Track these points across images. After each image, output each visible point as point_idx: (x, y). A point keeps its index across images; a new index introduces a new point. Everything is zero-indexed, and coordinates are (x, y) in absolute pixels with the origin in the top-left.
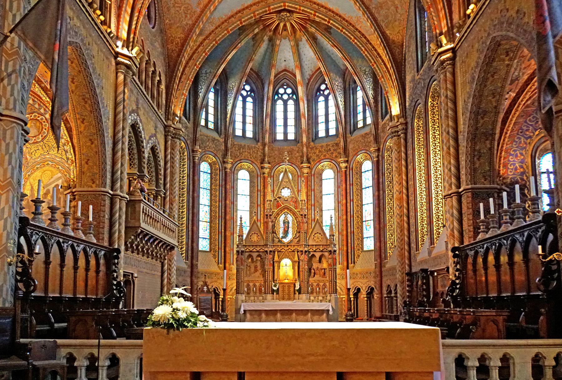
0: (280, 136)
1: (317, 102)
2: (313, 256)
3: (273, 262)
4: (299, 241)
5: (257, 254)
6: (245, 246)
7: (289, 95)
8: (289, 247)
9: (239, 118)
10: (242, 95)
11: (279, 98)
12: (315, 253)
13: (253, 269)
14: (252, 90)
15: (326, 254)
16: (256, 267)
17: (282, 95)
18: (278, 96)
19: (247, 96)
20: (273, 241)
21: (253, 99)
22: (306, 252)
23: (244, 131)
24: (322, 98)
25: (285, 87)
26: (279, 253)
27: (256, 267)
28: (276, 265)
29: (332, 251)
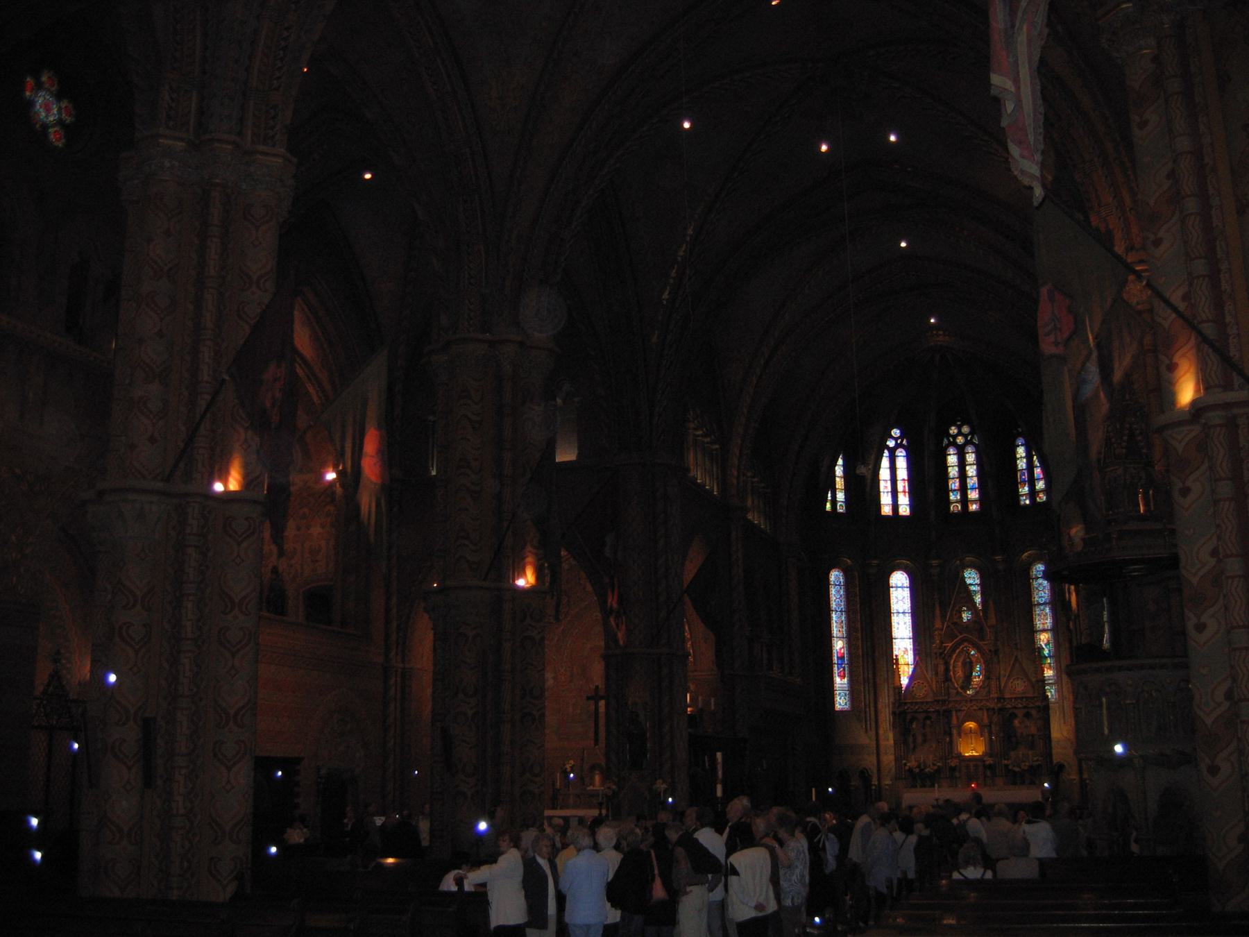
0: (956, 508)
2: (1013, 716)
3: (950, 728)
4: (989, 692)
6: (905, 704)
8: (974, 703)
9: (885, 486)
10: (888, 448)
13: (920, 739)
14: (902, 437)
17: (955, 437)
18: (949, 440)
19: (897, 446)
20: (948, 694)
22: (1000, 710)
23: (895, 506)
24: (1020, 441)
25: (959, 423)
26: (959, 714)
27: (925, 735)
28: (955, 731)
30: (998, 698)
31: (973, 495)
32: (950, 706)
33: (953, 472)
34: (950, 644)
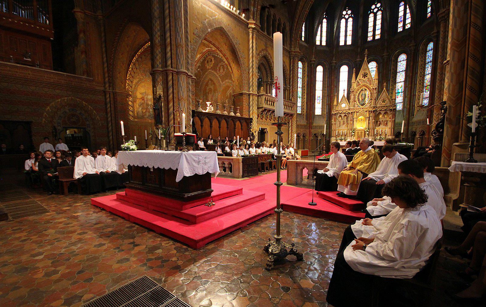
1: (399, 7)
2: (380, 113)
4: (371, 105)
5: (344, 114)
6: (337, 110)
7: (378, 8)
8: (364, 109)
11: (371, 13)
12: (381, 112)
13: (342, 123)
14: (351, 14)
15: (389, 112)
16: (344, 122)
18: (371, 11)
20: (354, 106)
21: (353, 19)
26: (357, 113)
27: (344, 122)
28: (355, 120)
29: (392, 109)
30: (373, 107)
31: (378, 32)
32: (354, 111)
33: (371, 24)
34: (357, 88)
